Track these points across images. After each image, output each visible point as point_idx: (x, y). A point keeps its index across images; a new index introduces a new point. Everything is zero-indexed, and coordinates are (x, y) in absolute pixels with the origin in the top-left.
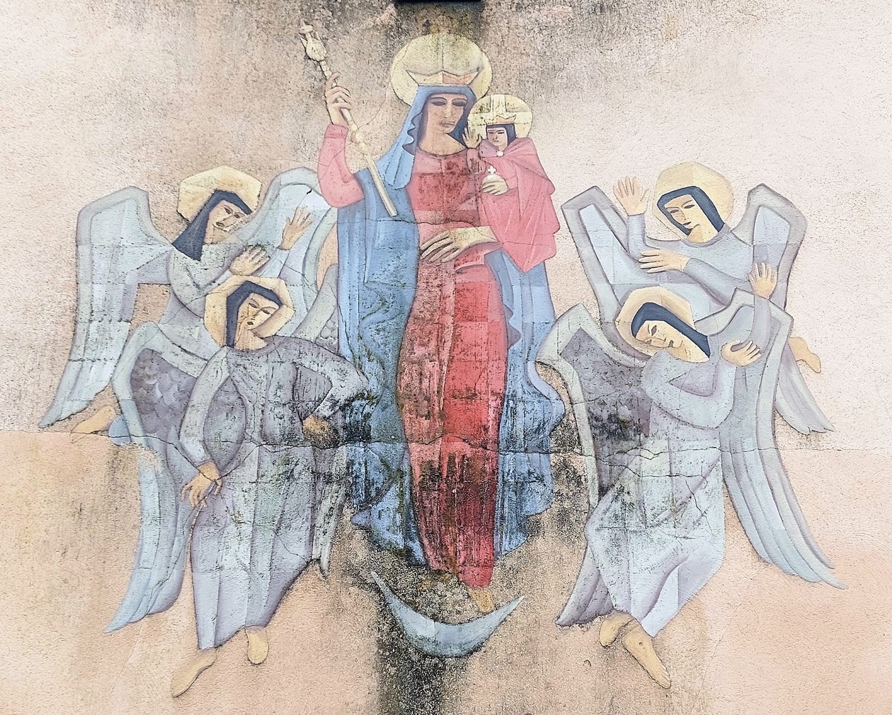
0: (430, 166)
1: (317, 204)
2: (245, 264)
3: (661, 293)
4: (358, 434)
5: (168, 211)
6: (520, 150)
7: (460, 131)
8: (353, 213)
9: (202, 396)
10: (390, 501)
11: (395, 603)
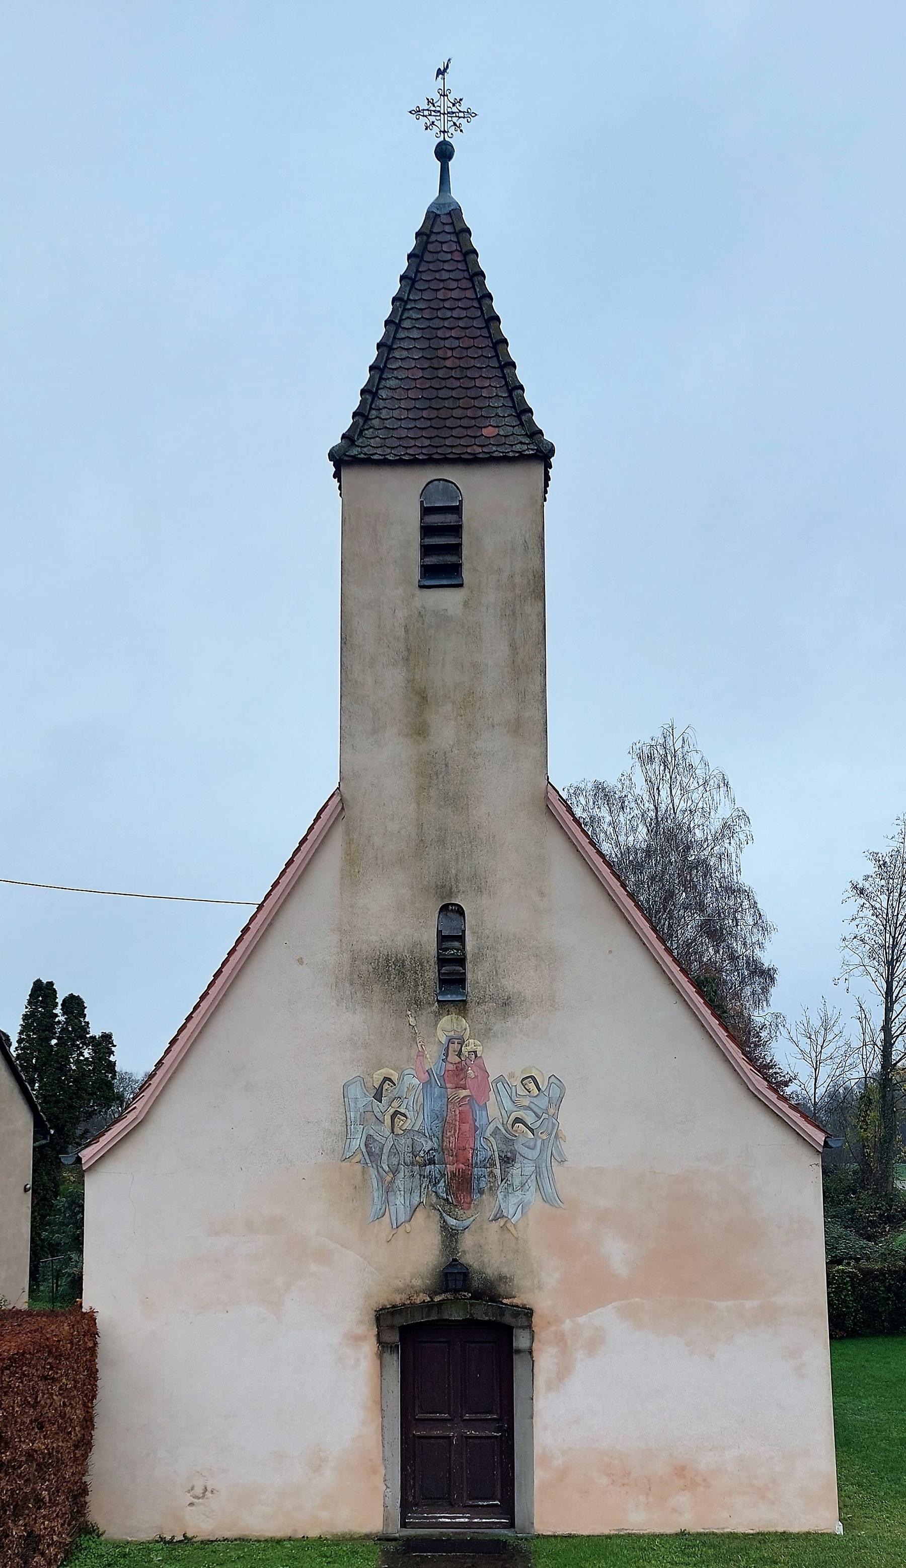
0: (450, 1067)
1: (416, 1081)
2: (395, 1104)
3: (521, 1114)
4: (432, 1162)
5: (369, 1085)
6: (478, 1061)
7: (459, 1054)
8: (427, 1084)
9: (386, 1151)
10: (442, 1184)
11: (444, 1215)
